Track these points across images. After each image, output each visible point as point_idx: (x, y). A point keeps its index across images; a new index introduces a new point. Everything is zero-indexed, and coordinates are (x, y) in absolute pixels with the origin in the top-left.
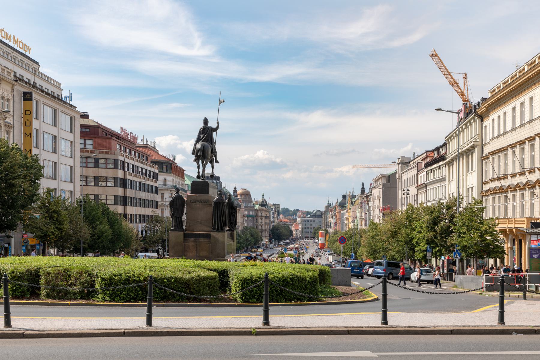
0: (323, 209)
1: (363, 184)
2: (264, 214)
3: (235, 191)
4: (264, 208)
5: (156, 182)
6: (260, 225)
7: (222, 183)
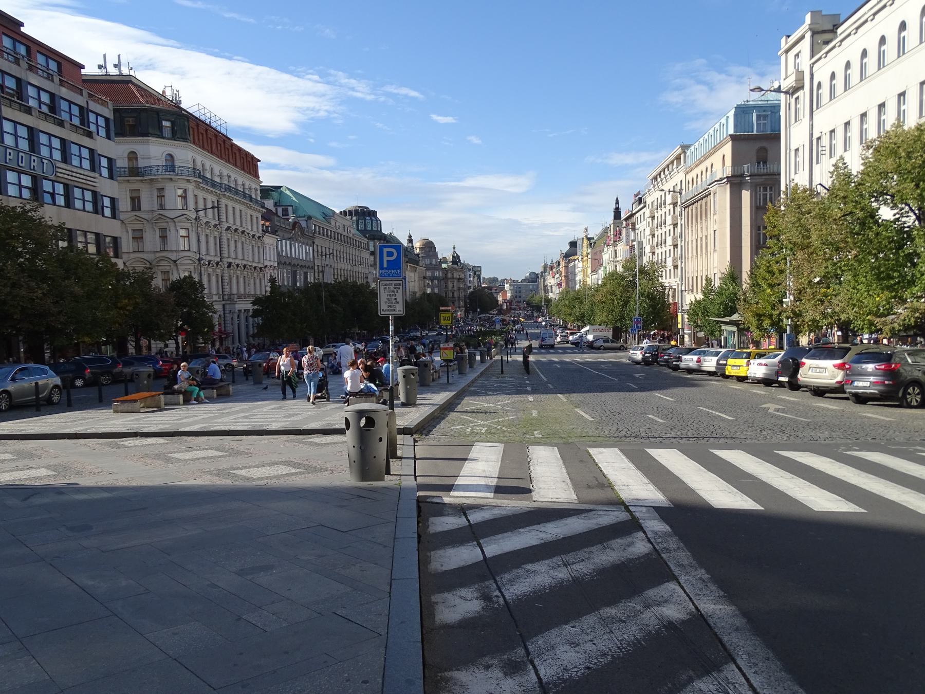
0: (539, 270)
1: (617, 202)
2: (456, 275)
3: (410, 241)
4: (456, 266)
5: (89, 135)
6: (451, 291)
7: (381, 222)
